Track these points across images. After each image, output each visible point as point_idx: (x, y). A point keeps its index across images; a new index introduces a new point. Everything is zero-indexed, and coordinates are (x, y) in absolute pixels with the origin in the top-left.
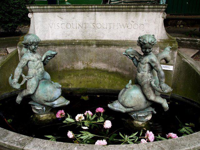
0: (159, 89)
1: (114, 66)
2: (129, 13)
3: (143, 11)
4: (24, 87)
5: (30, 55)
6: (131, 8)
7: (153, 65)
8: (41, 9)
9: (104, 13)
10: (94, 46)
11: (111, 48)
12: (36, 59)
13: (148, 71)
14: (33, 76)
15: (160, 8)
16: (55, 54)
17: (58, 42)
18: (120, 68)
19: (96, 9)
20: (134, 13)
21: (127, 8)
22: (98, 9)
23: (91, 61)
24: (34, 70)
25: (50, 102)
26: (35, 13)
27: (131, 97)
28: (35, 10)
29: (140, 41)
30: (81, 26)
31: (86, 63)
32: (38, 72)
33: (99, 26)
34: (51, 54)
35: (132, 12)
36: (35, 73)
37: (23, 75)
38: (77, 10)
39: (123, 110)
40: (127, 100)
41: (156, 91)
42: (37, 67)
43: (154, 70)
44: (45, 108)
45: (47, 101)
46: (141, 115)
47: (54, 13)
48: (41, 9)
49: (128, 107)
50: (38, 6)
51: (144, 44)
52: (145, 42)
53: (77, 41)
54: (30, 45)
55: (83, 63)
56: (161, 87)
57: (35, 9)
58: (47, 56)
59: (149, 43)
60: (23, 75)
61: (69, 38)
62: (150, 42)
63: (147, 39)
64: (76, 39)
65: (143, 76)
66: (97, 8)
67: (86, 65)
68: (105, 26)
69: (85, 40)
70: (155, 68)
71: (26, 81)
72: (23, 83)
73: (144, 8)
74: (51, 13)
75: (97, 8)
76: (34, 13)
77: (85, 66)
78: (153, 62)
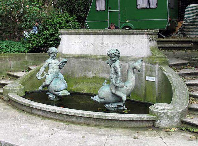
2: (124, 35)
3: (133, 34)
8: (67, 32)
10: (101, 60)
15: (143, 32)
32: (54, 71)
37: (45, 72)
39: (99, 100)
45: (56, 91)
46: (110, 106)
48: (67, 32)
53: (90, 56)
57: (63, 32)
60: (45, 72)
61: (85, 53)
69: (95, 55)
73: (133, 32)
77: (94, 75)
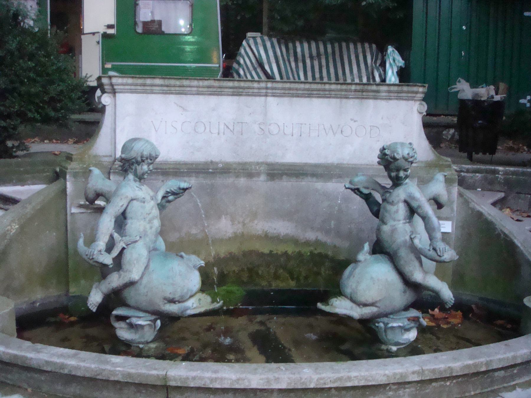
0: (432, 253)
1: (312, 228)
2: (344, 101)
3: (375, 98)
4: (118, 261)
5: (135, 187)
6: (351, 91)
7: (414, 204)
8: (136, 85)
9: (286, 100)
10: (263, 177)
11: (305, 183)
12: (148, 198)
13: (405, 219)
14: (140, 237)
15: (413, 92)
16: (187, 189)
17: (172, 166)
18: (327, 232)
19: (269, 91)
20: (357, 101)
21: (341, 90)
22: (274, 91)
23: (254, 215)
24: (142, 222)
25: (179, 302)
26: (121, 95)
27: (372, 278)
28: (122, 87)
29: (385, 155)
30: (231, 128)
31: (241, 220)
32: (151, 228)
33: (274, 129)
34: (180, 189)
35: (352, 98)
36: (145, 231)
37: (116, 235)
38: (223, 90)
39: (356, 313)
40: (362, 286)
41: (423, 259)
42: (151, 216)
43: (416, 216)
44: (161, 323)
45: (172, 301)
46: (395, 325)
47: (167, 95)
48: (136, 85)
49: (365, 305)
50: (133, 77)
51: (395, 159)
52: (397, 157)
53: (220, 165)
54: (138, 163)
55: (233, 221)
56: (435, 249)
57: (123, 84)
58: (167, 193)
59: (404, 158)
60: (116, 235)
61: (199, 157)
62: (406, 156)
63: (400, 151)
64: (217, 160)
65: (394, 231)
66: (272, 89)
67: (240, 226)
68: (288, 131)
69: (239, 164)
70: (419, 211)
71: (123, 249)
72: (115, 252)
73: (378, 91)
74: (160, 95)
75: (272, 89)
76: (117, 95)
77: (239, 229)
78: (413, 198)
